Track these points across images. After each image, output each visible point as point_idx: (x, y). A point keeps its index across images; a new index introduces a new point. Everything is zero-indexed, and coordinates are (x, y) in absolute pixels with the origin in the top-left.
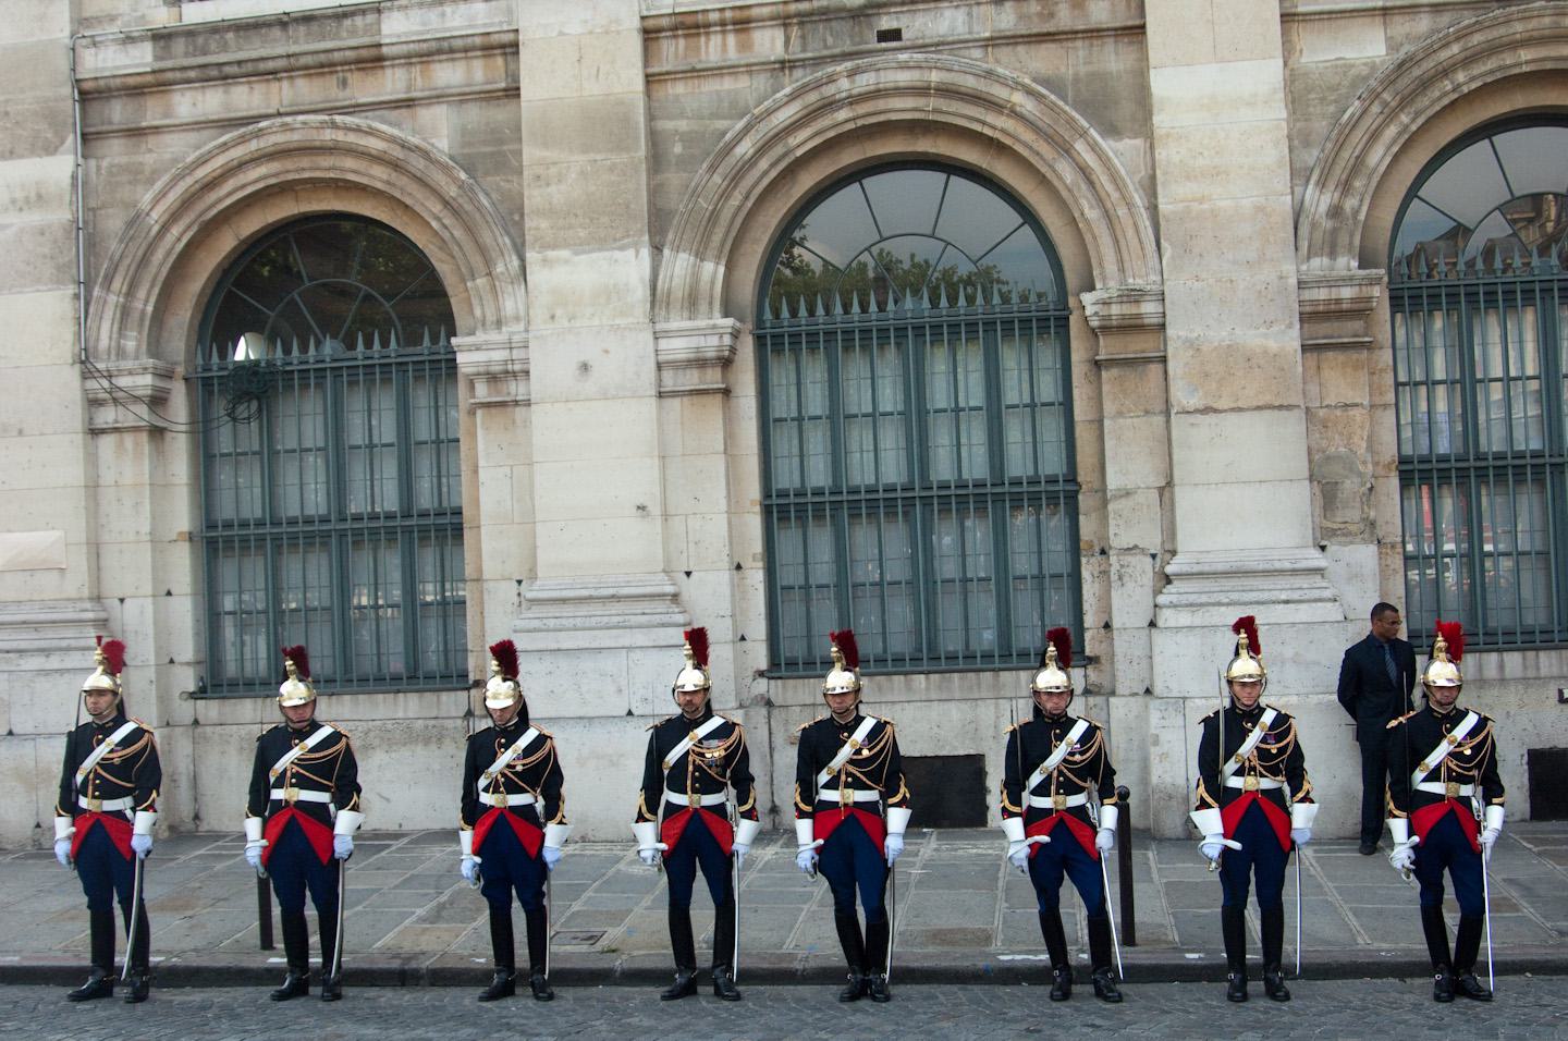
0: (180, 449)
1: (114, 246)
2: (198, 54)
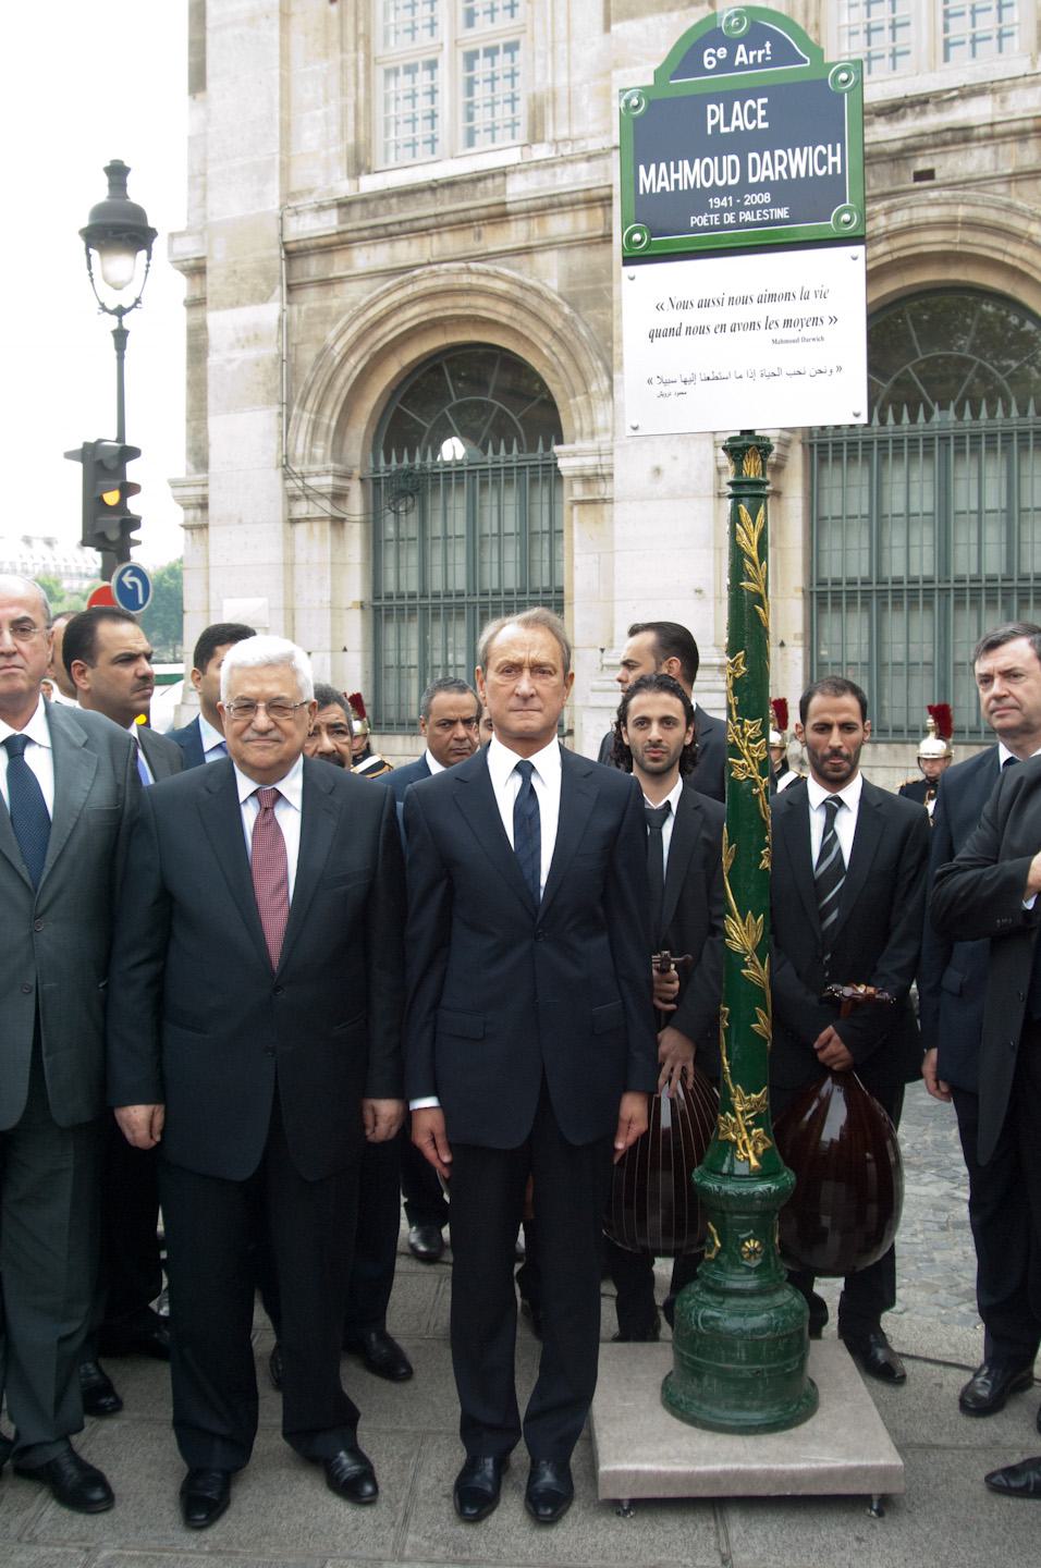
0: (355, 534)
1: (308, 374)
2: (372, 219)
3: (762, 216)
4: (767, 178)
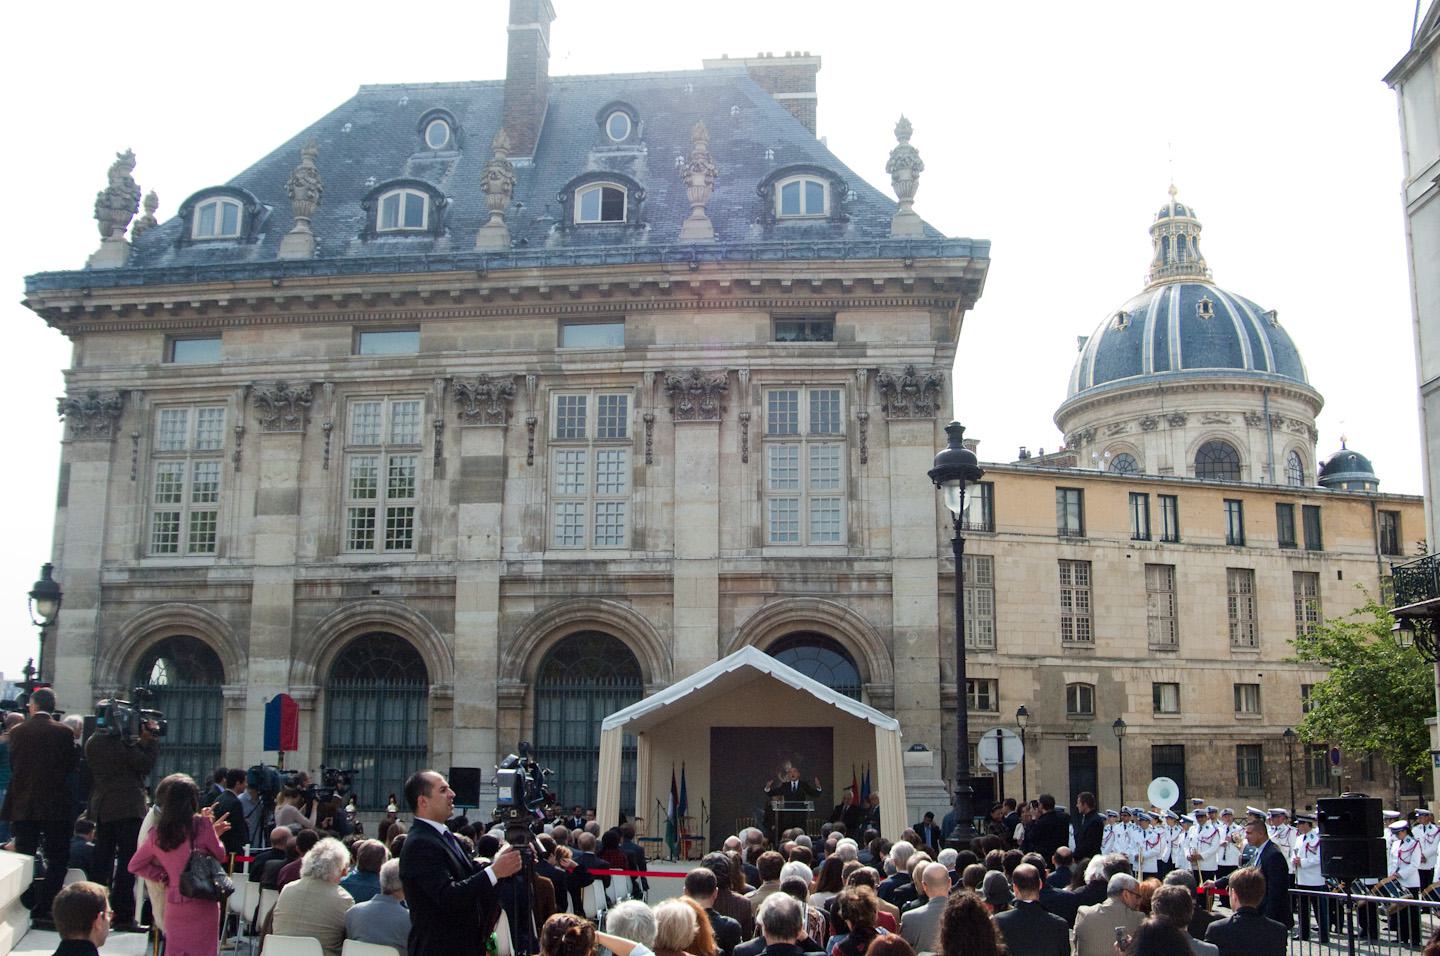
1: (108, 643)
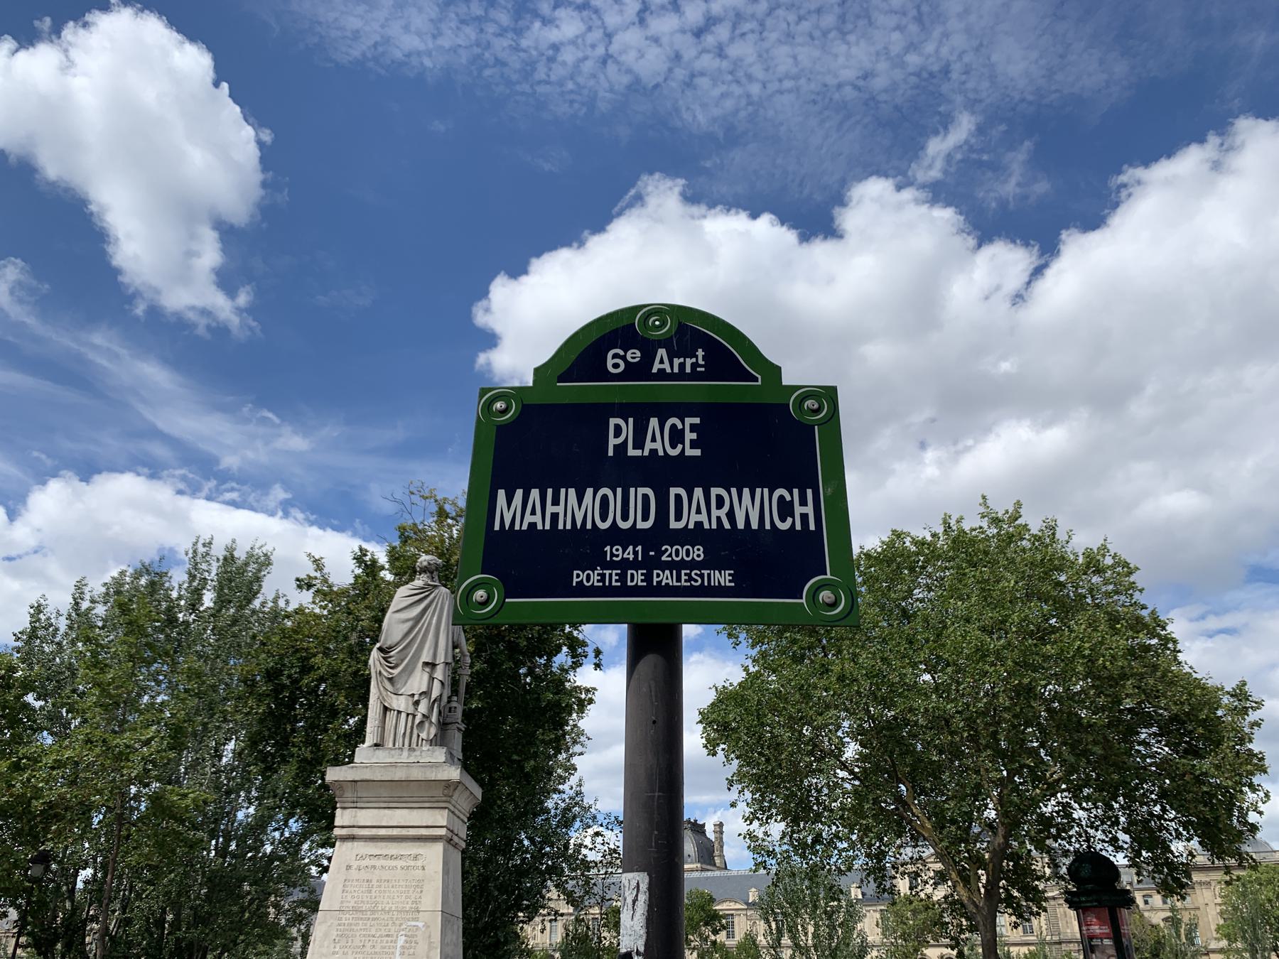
3: (690, 579)
4: (699, 524)
